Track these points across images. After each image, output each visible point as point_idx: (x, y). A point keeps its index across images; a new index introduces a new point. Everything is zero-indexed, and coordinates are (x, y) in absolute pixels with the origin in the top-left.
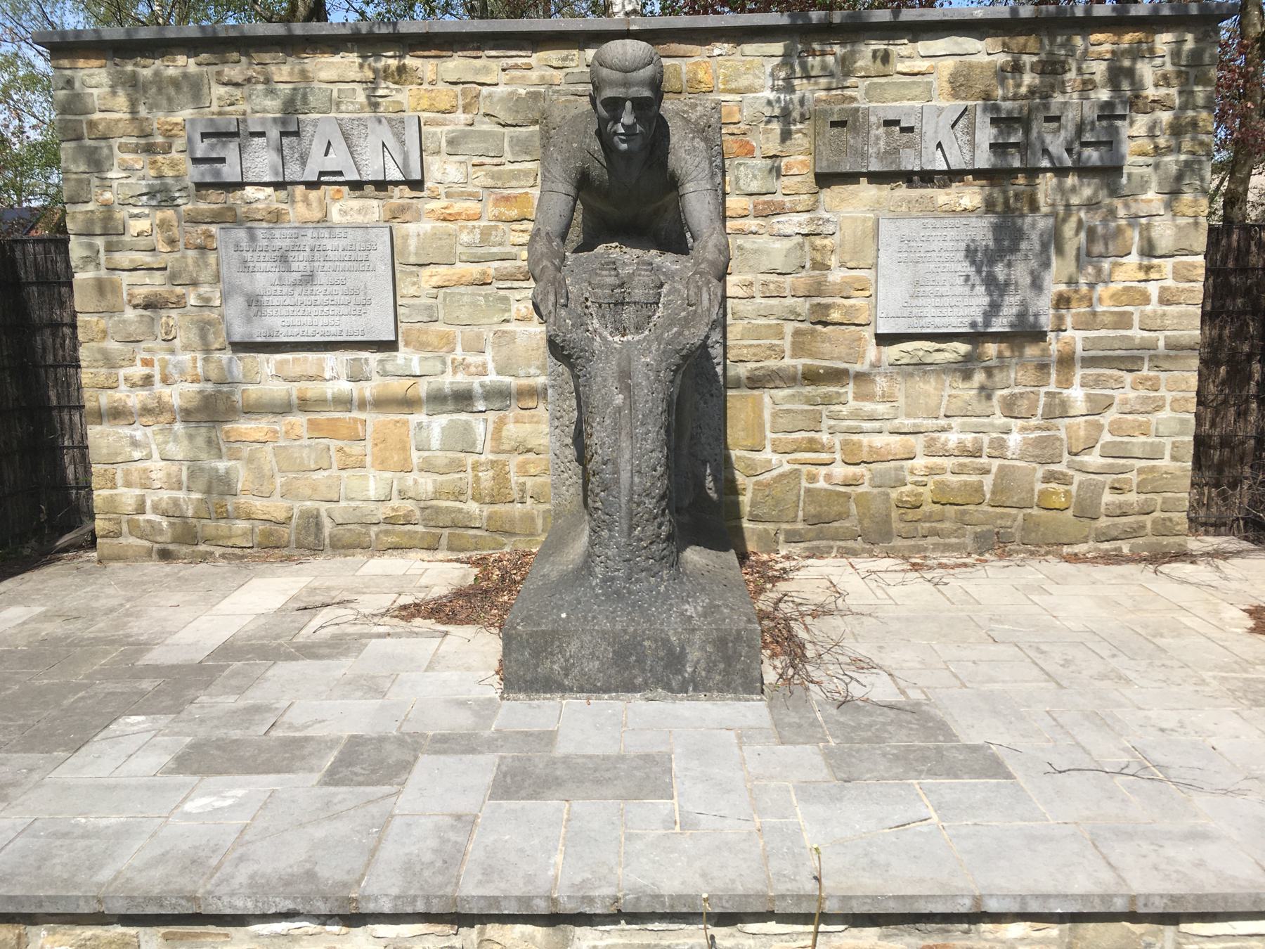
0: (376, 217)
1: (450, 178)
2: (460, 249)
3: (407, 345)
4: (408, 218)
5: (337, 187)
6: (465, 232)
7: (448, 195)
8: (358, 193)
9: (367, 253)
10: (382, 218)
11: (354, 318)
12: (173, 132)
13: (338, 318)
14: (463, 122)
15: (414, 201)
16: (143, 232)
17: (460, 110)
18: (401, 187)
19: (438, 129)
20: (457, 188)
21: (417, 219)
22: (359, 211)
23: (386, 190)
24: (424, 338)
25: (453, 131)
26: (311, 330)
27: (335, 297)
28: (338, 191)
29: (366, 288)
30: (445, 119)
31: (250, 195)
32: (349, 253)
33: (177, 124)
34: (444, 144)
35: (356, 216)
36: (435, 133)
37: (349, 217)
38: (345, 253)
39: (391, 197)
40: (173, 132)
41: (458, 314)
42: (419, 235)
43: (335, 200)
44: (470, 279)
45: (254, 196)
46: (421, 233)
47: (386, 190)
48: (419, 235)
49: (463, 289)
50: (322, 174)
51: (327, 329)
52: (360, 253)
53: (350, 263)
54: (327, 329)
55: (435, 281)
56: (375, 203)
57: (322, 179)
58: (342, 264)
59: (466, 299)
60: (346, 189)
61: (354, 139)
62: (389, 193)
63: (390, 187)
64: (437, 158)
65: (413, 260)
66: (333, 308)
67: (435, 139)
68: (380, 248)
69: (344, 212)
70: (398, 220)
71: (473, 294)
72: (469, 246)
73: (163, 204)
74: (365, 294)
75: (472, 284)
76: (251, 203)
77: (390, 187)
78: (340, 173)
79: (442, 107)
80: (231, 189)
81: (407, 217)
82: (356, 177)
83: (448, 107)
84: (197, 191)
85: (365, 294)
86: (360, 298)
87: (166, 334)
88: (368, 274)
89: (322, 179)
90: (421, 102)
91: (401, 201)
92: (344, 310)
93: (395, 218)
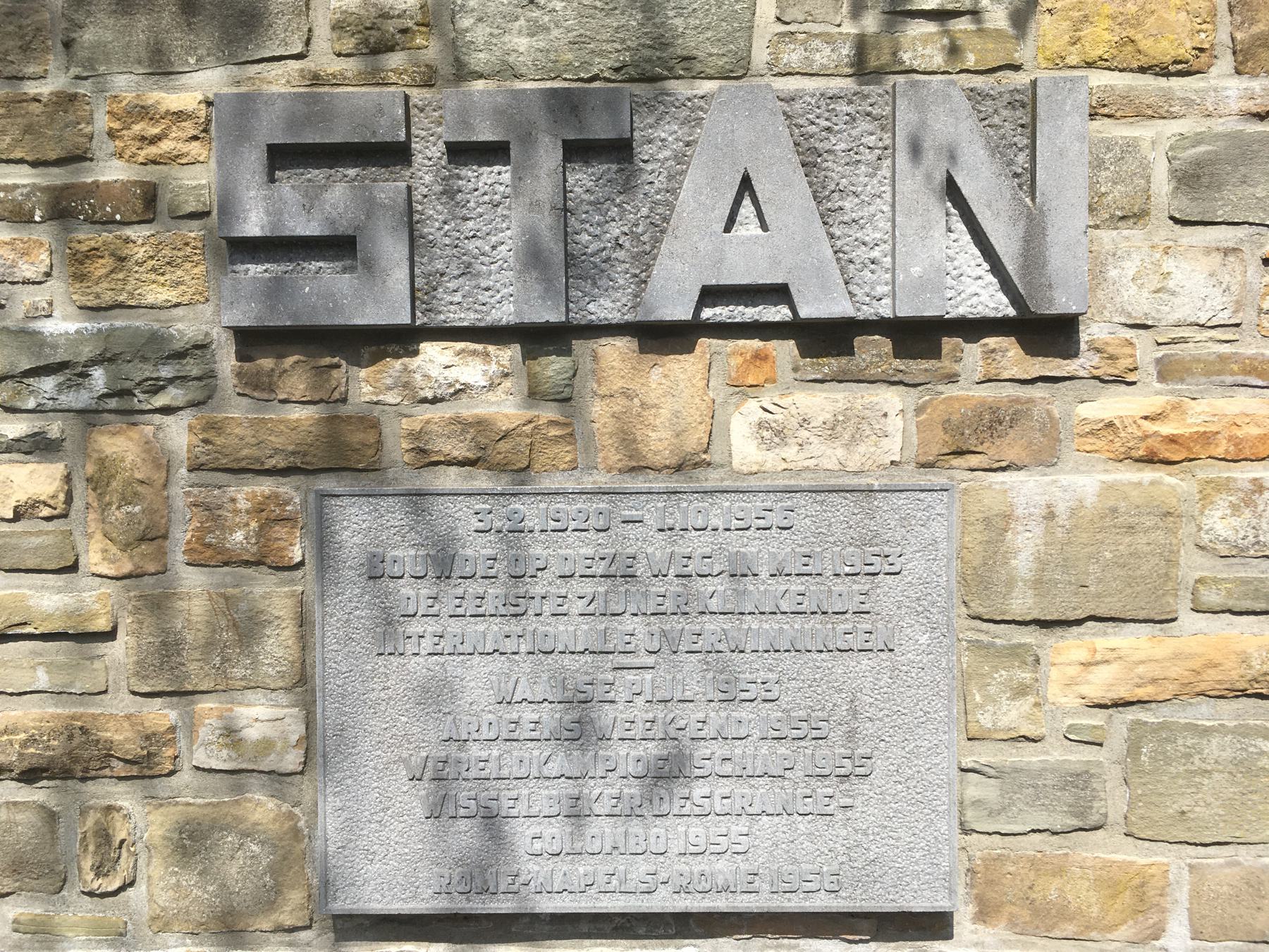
0: (892, 448)
1: (1183, 310)
2: (1192, 566)
3: (984, 913)
4: (1010, 455)
5: (756, 344)
6: (1222, 503)
7: (1167, 371)
8: (831, 365)
9: (863, 584)
10: (911, 453)
11: (803, 825)
12: (166, 146)
13: (742, 825)
14: (1235, 106)
15: (1038, 391)
16: (35, 504)
17: (1226, 63)
18: (992, 342)
19: (1143, 132)
20: (1206, 347)
21: (1046, 458)
22: (832, 430)
23: (936, 354)
24: (1051, 889)
25: (1198, 139)
26: (642, 867)
27: (738, 749)
28: (759, 357)
29: (854, 713)
30: (1168, 97)
31: (435, 372)
32: (796, 586)
33: (180, 116)
34: (1162, 183)
35: (817, 447)
36: (1131, 146)
37: (791, 452)
38: (780, 585)
39: (952, 378)
40: (166, 146)
41: (1184, 803)
42: (1051, 516)
43: (742, 389)
44: (1234, 674)
45: (452, 374)
46: (1061, 509)
47: (936, 354)
48: (1051, 516)
49: (1203, 713)
50: (711, 295)
51: (698, 865)
52: (840, 586)
53: (798, 622)
54: (698, 865)
55: (1101, 684)
56: (891, 399)
57: (707, 313)
58: (770, 625)
59: (1215, 748)
60: (785, 350)
61: (835, 170)
62: (946, 364)
63: (948, 343)
64: (1132, 235)
65: (1022, 604)
66: (724, 787)
67: (1131, 165)
68: (915, 566)
69: (771, 434)
70: (973, 461)
71: (1243, 732)
72: (1236, 553)
73: (113, 403)
74: (851, 735)
75: (1244, 694)
76: (435, 401)
77: (948, 343)
78: (780, 293)
79: (1164, 50)
80: (366, 352)
81: (1010, 450)
82: (839, 307)
83: (1182, 53)
84: (241, 357)
85: (851, 735)
86: (831, 753)
87: (99, 871)
88: (865, 661)
89: (707, 313)
90: (1086, 31)
91: (987, 393)
92: (763, 793)
93: (960, 453)
